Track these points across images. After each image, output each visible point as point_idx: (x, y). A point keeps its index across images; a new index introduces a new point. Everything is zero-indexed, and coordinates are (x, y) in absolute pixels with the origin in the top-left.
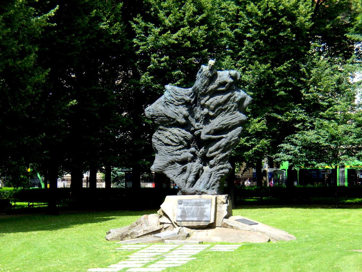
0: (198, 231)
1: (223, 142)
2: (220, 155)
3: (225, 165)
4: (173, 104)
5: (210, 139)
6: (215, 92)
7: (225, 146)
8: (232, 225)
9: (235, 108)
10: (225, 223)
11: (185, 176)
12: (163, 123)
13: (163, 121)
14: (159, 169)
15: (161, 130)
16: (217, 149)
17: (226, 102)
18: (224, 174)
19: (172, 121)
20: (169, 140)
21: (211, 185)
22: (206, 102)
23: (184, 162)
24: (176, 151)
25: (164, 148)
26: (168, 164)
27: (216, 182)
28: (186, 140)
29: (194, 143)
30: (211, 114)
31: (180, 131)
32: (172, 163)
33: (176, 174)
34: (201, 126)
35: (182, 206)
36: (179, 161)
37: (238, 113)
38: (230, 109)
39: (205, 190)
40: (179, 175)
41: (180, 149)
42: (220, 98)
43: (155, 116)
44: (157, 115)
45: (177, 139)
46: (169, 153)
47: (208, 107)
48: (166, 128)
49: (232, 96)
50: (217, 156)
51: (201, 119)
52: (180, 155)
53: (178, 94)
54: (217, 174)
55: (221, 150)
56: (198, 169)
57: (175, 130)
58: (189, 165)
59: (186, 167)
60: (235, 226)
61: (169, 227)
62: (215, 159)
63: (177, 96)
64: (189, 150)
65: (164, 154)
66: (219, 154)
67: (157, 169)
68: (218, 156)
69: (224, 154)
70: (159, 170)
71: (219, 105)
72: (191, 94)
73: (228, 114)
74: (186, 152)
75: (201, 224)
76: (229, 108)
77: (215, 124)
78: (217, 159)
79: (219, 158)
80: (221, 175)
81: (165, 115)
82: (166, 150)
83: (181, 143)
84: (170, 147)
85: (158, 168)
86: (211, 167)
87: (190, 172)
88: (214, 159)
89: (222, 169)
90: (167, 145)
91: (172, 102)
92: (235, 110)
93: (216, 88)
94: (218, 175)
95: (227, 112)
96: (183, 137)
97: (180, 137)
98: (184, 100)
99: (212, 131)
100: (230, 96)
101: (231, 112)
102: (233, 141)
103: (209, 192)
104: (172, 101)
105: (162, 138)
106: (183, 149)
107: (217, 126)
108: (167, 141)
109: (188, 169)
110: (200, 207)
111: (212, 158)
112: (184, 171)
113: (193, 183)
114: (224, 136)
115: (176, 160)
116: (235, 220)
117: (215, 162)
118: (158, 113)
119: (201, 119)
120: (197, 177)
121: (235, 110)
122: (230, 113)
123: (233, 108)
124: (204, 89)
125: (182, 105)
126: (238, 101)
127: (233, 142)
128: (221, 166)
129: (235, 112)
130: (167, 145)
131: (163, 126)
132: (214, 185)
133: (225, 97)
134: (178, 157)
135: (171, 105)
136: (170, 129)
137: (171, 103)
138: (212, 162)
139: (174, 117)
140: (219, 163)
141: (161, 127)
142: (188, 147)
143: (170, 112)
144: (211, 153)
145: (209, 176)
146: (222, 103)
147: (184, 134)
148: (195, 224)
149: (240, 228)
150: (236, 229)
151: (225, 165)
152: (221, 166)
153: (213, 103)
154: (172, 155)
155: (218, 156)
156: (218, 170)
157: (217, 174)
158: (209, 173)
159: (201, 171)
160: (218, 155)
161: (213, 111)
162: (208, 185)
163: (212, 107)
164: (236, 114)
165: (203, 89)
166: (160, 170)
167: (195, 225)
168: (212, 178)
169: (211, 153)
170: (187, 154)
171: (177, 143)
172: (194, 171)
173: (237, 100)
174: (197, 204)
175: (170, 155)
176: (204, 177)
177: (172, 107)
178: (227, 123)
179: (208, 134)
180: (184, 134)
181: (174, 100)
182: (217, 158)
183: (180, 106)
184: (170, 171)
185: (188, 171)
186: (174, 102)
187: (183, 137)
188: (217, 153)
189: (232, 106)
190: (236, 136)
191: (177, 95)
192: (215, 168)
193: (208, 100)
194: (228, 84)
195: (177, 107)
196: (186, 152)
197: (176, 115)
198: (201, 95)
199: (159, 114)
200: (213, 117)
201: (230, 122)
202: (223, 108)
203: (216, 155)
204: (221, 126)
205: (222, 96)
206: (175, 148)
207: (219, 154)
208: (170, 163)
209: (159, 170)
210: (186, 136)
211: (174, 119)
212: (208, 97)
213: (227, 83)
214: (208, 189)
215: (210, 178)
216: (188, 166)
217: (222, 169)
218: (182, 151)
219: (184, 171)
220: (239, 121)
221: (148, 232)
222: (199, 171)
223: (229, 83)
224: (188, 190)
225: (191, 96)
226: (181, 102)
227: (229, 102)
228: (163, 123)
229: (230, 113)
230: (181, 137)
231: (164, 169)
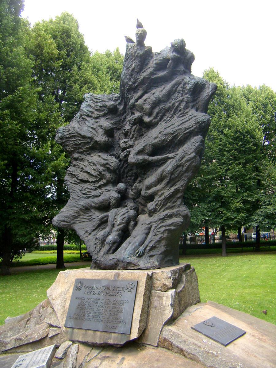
0: (105, 358)
1: (168, 167)
2: (166, 191)
3: (175, 210)
4: (91, 117)
5: (144, 161)
6: (151, 83)
7: (172, 173)
8: (182, 346)
9: (187, 103)
10: (165, 340)
11: (101, 234)
12: (77, 147)
13: (76, 145)
14: (64, 221)
15: (76, 159)
16: (160, 180)
17: (169, 95)
18: (175, 226)
19: (88, 143)
20: (85, 174)
21: (148, 248)
22: (137, 100)
23: (105, 207)
24: (95, 190)
25: (78, 187)
26: (78, 212)
27: (159, 241)
28: (109, 170)
29: (127, 177)
30: (147, 119)
31: (99, 156)
32: (86, 209)
33: (89, 229)
34: (130, 143)
35: (80, 293)
36: (97, 206)
37: (193, 112)
38: (178, 106)
39: (134, 259)
40: (94, 230)
41: (100, 187)
42: (158, 92)
43: (67, 138)
44: (68, 136)
45: (95, 170)
46: (84, 194)
47: (141, 109)
48: (83, 156)
49: (180, 83)
50: (160, 193)
51: (132, 133)
52: (99, 196)
53: (98, 101)
54: (160, 228)
55: (166, 181)
56: (125, 219)
57: (95, 157)
58: (111, 214)
59: (107, 216)
60: (189, 351)
61: (59, 336)
62: (157, 198)
63: (96, 104)
64: (115, 189)
65: (76, 197)
66: (163, 188)
67: (62, 221)
68: (162, 194)
69: (173, 189)
70: (65, 223)
71: (157, 103)
72: (119, 97)
73: (176, 116)
74: (109, 191)
75: (110, 338)
76: (177, 104)
77: (154, 136)
78: (160, 199)
79: (163, 197)
80: (167, 228)
81: (78, 134)
82: (80, 191)
83: (101, 176)
84: (87, 185)
85: (63, 219)
86: (151, 213)
87: (113, 225)
88: (155, 200)
89: (170, 216)
90: (83, 181)
91: (90, 114)
92: (186, 107)
93: (152, 73)
94: (163, 229)
95: (174, 114)
96: (104, 165)
97: (98, 166)
98: (106, 106)
99: (149, 149)
100: (177, 84)
101: (180, 111)
102: (187, 161)
103: (142, 263)
104: (90, 111)
105: (77, 172)
106: (105, 185)
107: (156, 138)
108: (82, 176)
109: (110, 219)
110: (112, 298)
111: (151, 198)
112: (103, 223)
113: (117, 245)
114: (170, 155)
115: (93, 204)
116: (192, 328)
117: (156, 205)
118: (69, 132)
119: (132, 133)
120: (125, 234)
121: (186, 107)
122: (180, 113)
123: (184, 104)
124: (132, 80)
125: (104, 115)
126: (190, 89)
127: (188, 164)
128: (168, 212)
129: (187, 110)
130: (83, 181)
131: (78, 153)
132: (153, 248)
133: (168, 86)
134: (96, 200)
135: (88, 119)
136: (89, 158)
137: (88, 116)
138: (151, 205)
139: (89, 135)
140: (165, 204)
141: (76, 155)
142: (115, 183)
143: (86, 128)
144: (148, 188)
145: (147, 231)
146: (163, 97)
147: (104, 160)
148: (98, 339)
149: (201, 359)
150: (191, 359)
151: (175, 210)
152: (168, 212)
153: (149, 101)
154: (89, 197)
155: (162, 194)
156: (163, 219)
157: (160, 228)
158: (147, 226)
159: (132, 223)
160: (162, 192)
161: (150, 115)
162: (141, 249)
163: (147, 107)
164: (190, 113)
165: (130, 79)
166: (67, 222)
167: (98, 342)
168: (151, 234)
169: (148, 188)
170: (111, 193)
171: (96, 176)
172: (118, 222)
173: (188, 87)
174: (111, 290)
175: (85, 198)
176: (137, 234)
177: (91, 121)
178: (174, 130)
179: (140, 152)
180: (104, 160)
181: (93, 111)
182: (160, 197)
183: (102, 119)
184: (81, 224)
185: (109, 223)
186: (93, 112)
187: (104, 165)
188: (159, 187)
189: (182, 101)
190: (191, 151)
191: (97, 102)
192: (157, 217)
193: (140, 97)
194: (170, 61)
195: (98, 120)
196: (109, 191)
197: (93, 131)
198: (129, 90)
199: (70, 134)
200: (150, 126)
201: (180, 127)
202: (167, 107)
203: (158, 191)
204: (163, 138)
205: (163, 87)
206: (92, 186)
207: (163, 188)
208: (81, 210)
209: (65, 223)
210: (107, 164)
211: (91, 138)
212: (139, 93)
213: (168, 60)
214: (140, 256)
215: (147, 234)
216: (109, 215)
217: (170, 216)
218: (103, 189)
219: (103, 223)
220: (196, 124)
221: (21, 344)
222: (128, 222)
223: (172, 59)
224: (102, 259)
225: (119, 101)
226: (103, 111)
227: (176, 94)
228: (77, 147)
229: (180, 113)
230: (101, 166)
231: (72, 222)
